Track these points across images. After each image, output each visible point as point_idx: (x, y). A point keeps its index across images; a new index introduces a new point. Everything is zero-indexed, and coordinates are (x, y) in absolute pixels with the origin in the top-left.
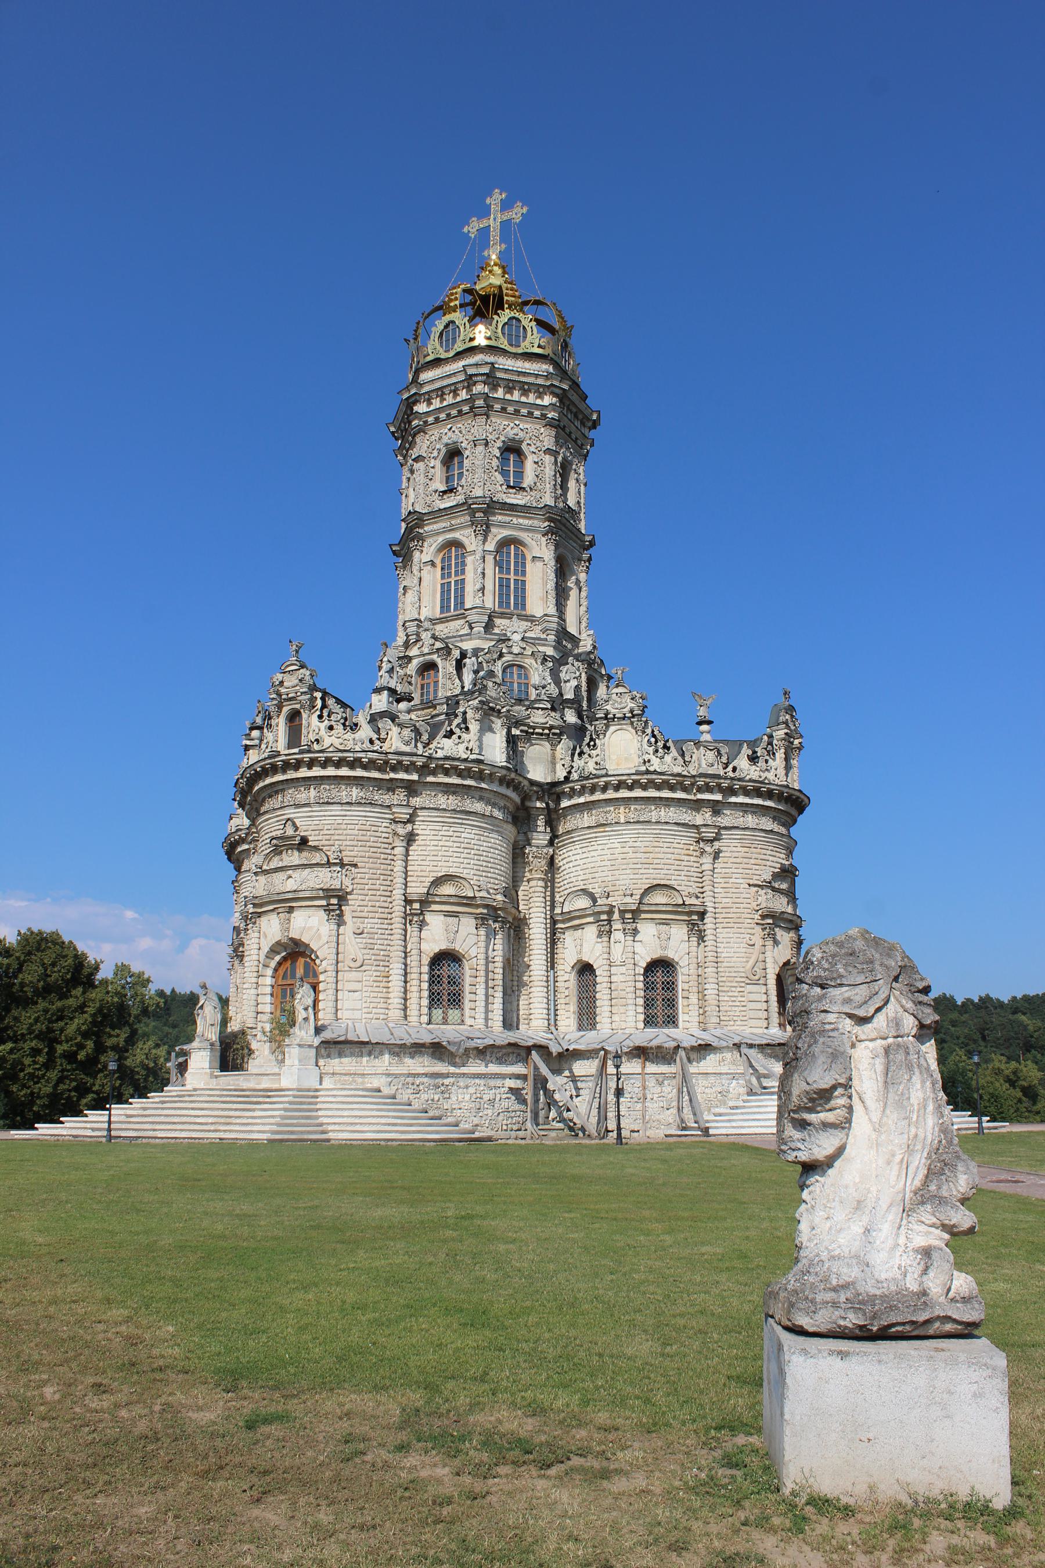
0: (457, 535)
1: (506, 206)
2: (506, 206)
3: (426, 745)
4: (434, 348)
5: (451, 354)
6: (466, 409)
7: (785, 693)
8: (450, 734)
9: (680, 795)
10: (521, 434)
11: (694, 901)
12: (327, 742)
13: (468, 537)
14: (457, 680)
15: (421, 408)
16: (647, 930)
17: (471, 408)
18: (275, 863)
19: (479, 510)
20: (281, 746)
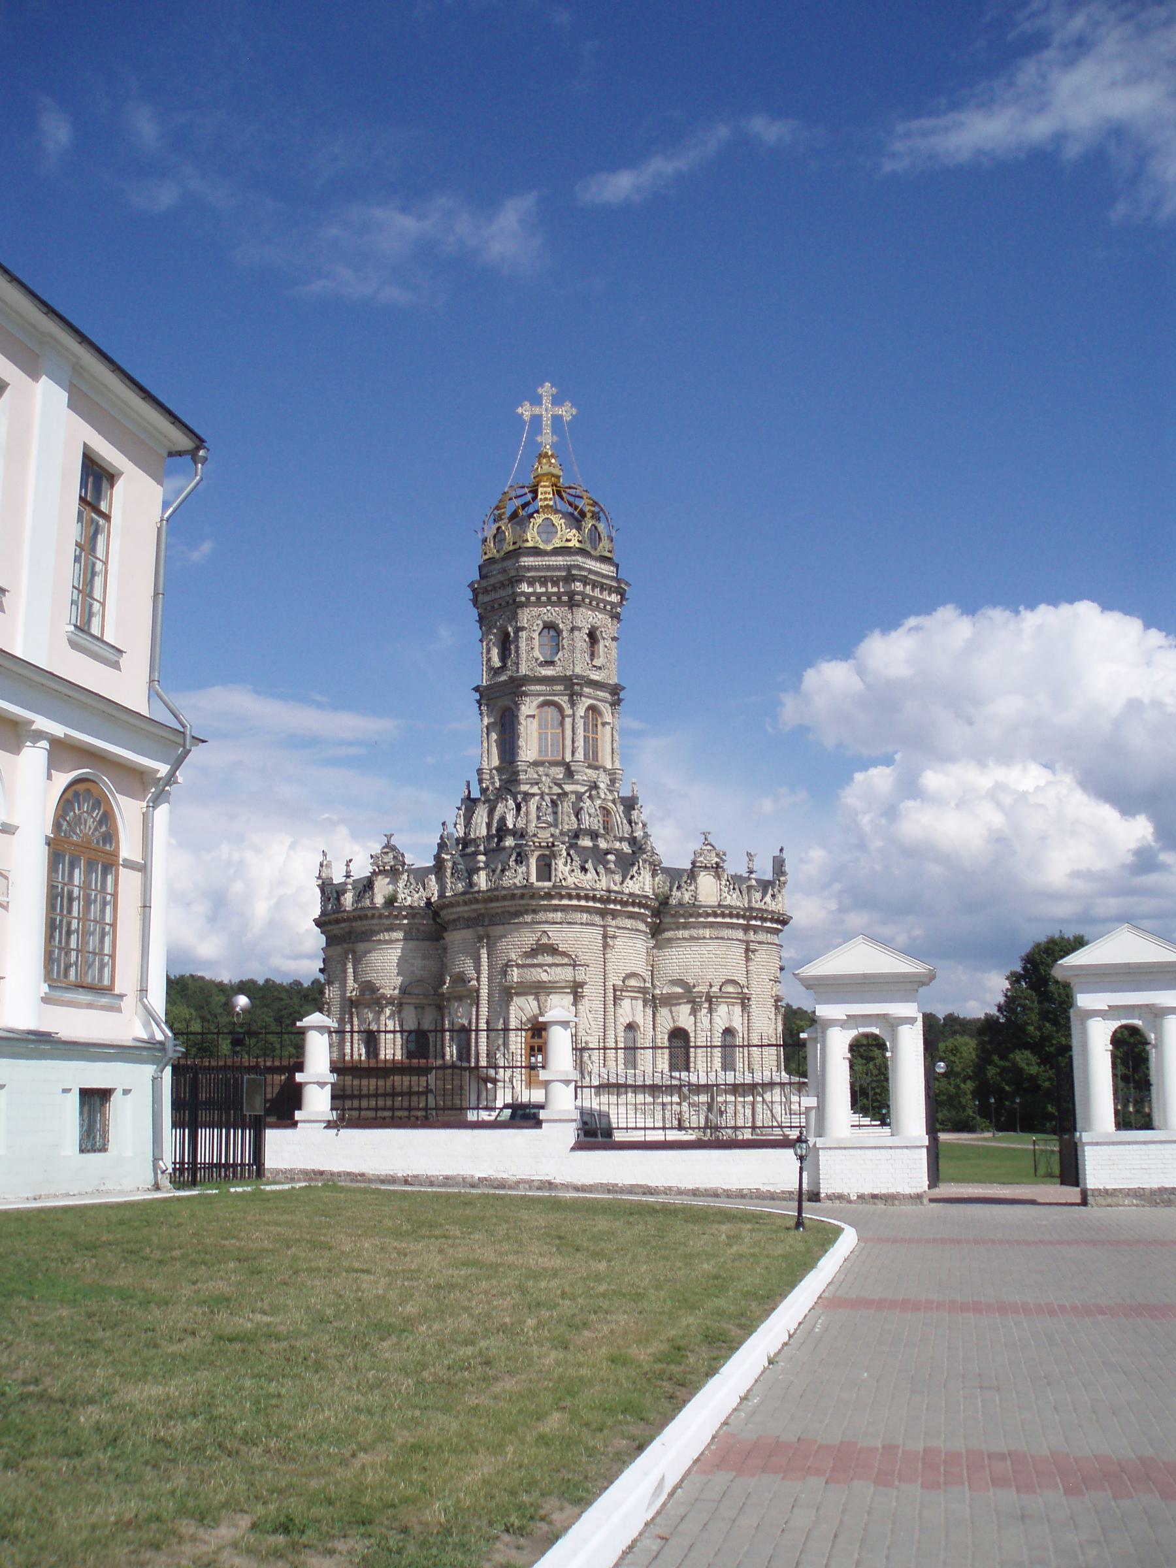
0: (556, 698)
1: (557, 401)
2: (557, 401)
3: (622, 882)
4: (532, 537)
5: (549, 548)
6: (565, 598)
7: (781, 850)
8: (632, 877)
9: (741, 921)
10: (599, 624)
11: (746, 991)
12: (571, 881)
13: (563, 701)
14: (573, 818)
15: (525, 588)
16: (722, 1010)
17: (571, 598)
18: (529, 961)
19: (577, 684)
20: (533, 878)
